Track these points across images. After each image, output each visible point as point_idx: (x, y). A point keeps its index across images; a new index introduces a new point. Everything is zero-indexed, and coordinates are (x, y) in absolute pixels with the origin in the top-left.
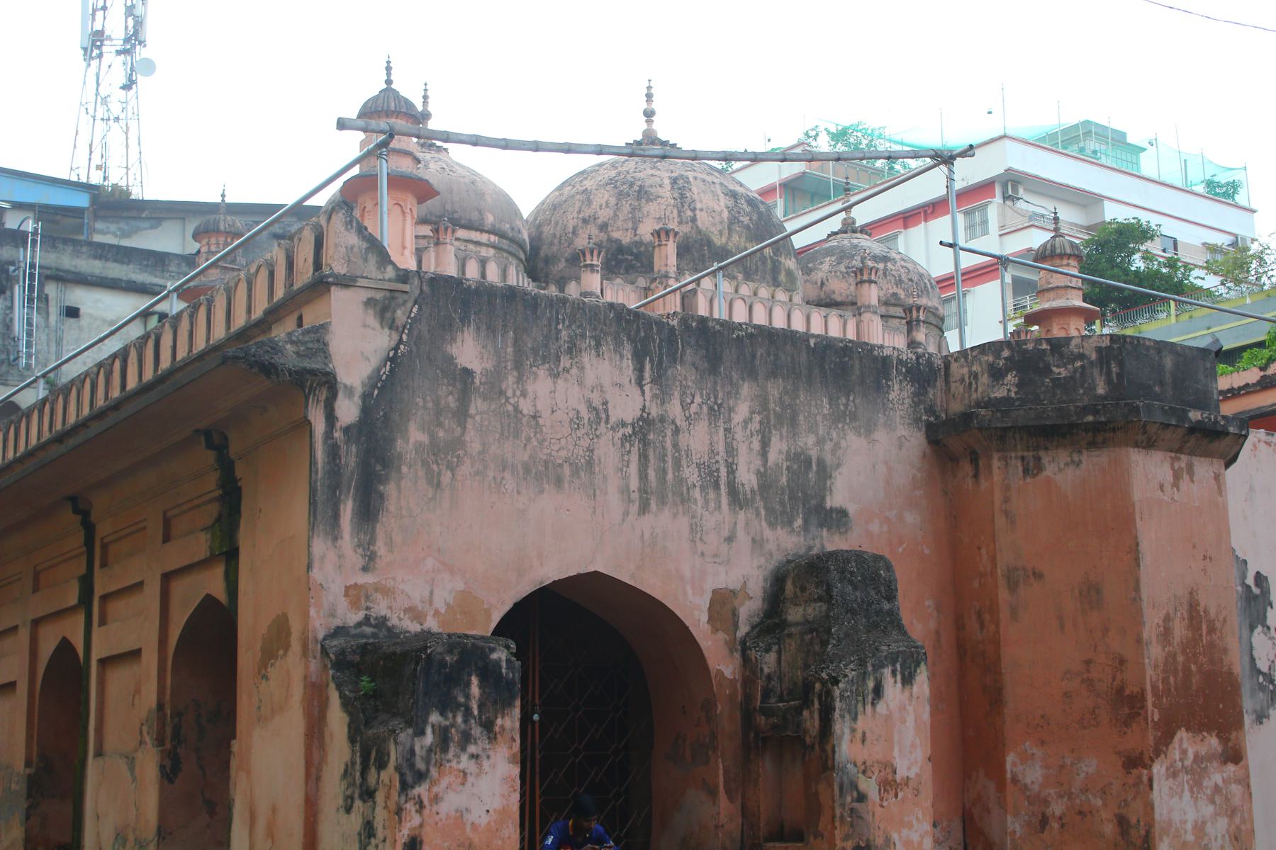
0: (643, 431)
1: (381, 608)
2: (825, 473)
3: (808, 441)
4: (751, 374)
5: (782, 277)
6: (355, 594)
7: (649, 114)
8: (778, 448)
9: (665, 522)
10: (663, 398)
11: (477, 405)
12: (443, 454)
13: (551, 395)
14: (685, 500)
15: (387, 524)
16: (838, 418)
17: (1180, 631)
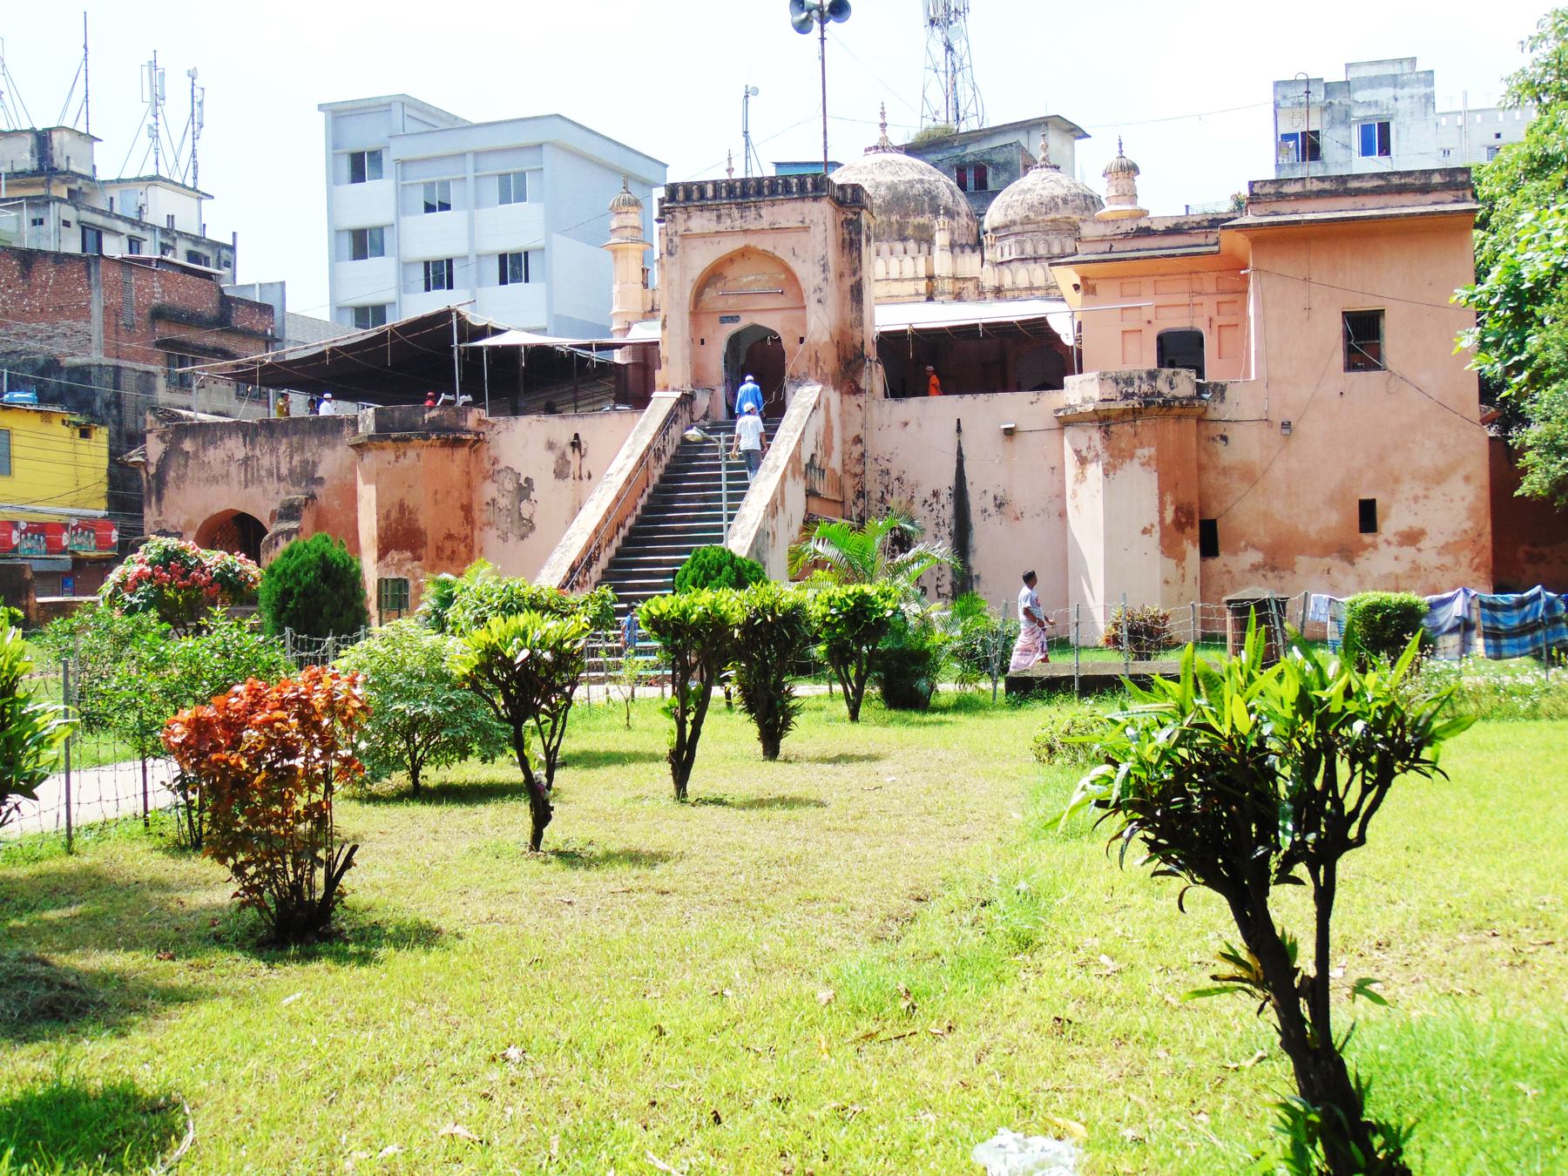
0: (247, 459)
1: (164, 526)
2: (315, 464)
3: (308, 455)
4: (286, 434)
5: (910, 231)
6: (157, 523)
7: (883, 125)
8: (296, 459)
9: (254, 490)
10: (253, 449)
11: (191, 462)
12: (181, 478)
13: (214, 455)
14: (261, 482)
15: (165, 502)
16: (321, 444)
17: (394, 515)
